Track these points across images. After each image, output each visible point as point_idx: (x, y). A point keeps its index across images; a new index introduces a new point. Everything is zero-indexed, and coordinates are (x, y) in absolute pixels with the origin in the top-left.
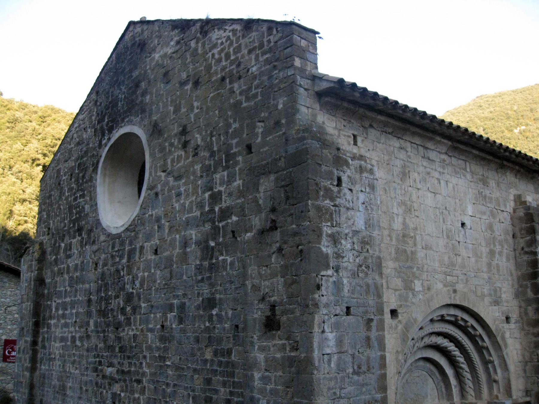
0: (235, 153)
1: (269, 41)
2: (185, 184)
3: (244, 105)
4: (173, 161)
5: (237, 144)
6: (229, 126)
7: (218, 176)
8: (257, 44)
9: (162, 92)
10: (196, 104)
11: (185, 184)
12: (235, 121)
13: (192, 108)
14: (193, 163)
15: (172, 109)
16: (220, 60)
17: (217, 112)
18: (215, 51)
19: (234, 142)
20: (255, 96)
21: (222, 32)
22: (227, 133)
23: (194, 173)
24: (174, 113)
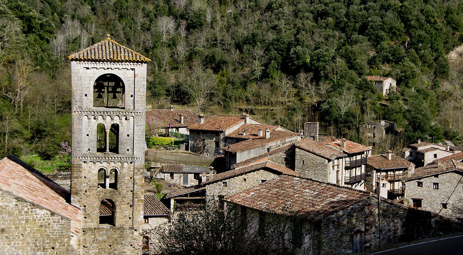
0: (47, 249)
1: (62, 222)
2: (21, 252)
3: (51, 236)
4: (15, 244)
5: (48, 246)
6: (45, 240)
7: (39, 252)
8: (57, 221)
9: (6, 219)
10: (27, 229)
11: (21, 252)
12: (47, 240)
13: (26, 230)
14: (26, 247)
15: (14, 227)
16: (40, 220)
17: (39, 235)
18: (38, 216)
19: (47, 245)
20: (56, 235)
21: (41, 211)
22: (44, 242)
23: (27, 249)
24: (15, 228)
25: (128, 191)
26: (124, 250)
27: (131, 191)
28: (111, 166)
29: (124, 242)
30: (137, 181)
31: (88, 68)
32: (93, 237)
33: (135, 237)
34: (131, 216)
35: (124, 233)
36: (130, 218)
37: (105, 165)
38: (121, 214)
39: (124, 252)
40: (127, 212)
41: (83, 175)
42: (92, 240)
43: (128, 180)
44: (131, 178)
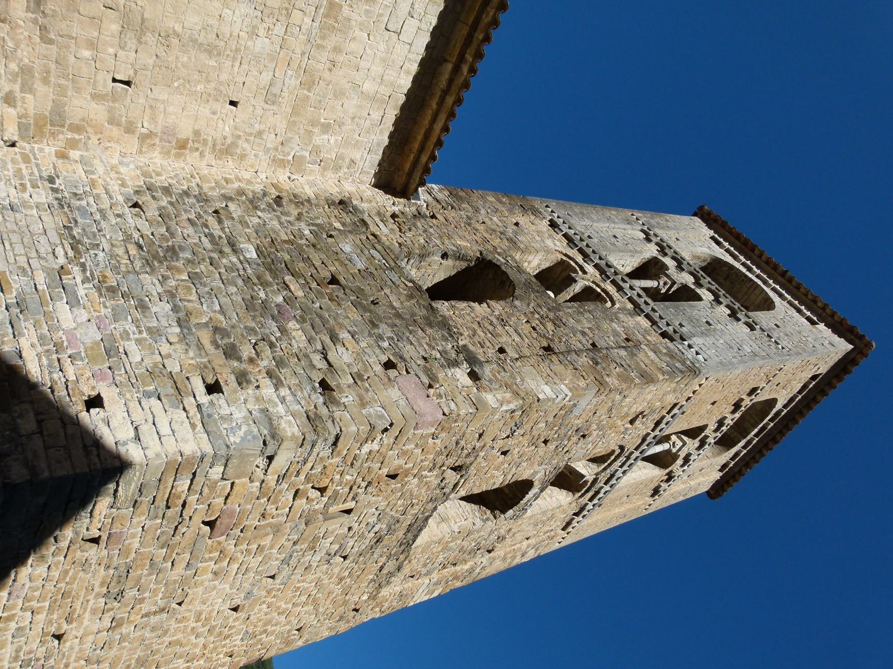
25: (583, 334)
26: (344, 335)
27: (593, 345)
28: (603, 285)
29: (384, 329)
30: (641, 356)
31: (718, 243)
32: (337, 225)
33: (441, 375)
34: (512, 353)
35: (429, 331)
36: (502, 350)
37: (589, 268)
38: (495, 321)
39: (334, 338)
40: (517, 339)
41: (523, 220)
42: (319, 221)
43: (616, 334)
44: (628, 340)
